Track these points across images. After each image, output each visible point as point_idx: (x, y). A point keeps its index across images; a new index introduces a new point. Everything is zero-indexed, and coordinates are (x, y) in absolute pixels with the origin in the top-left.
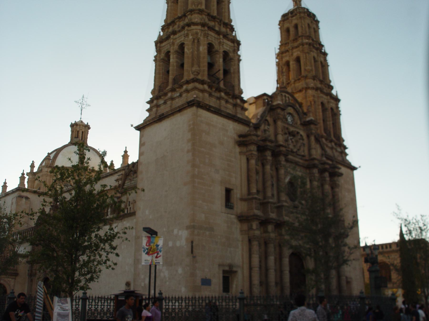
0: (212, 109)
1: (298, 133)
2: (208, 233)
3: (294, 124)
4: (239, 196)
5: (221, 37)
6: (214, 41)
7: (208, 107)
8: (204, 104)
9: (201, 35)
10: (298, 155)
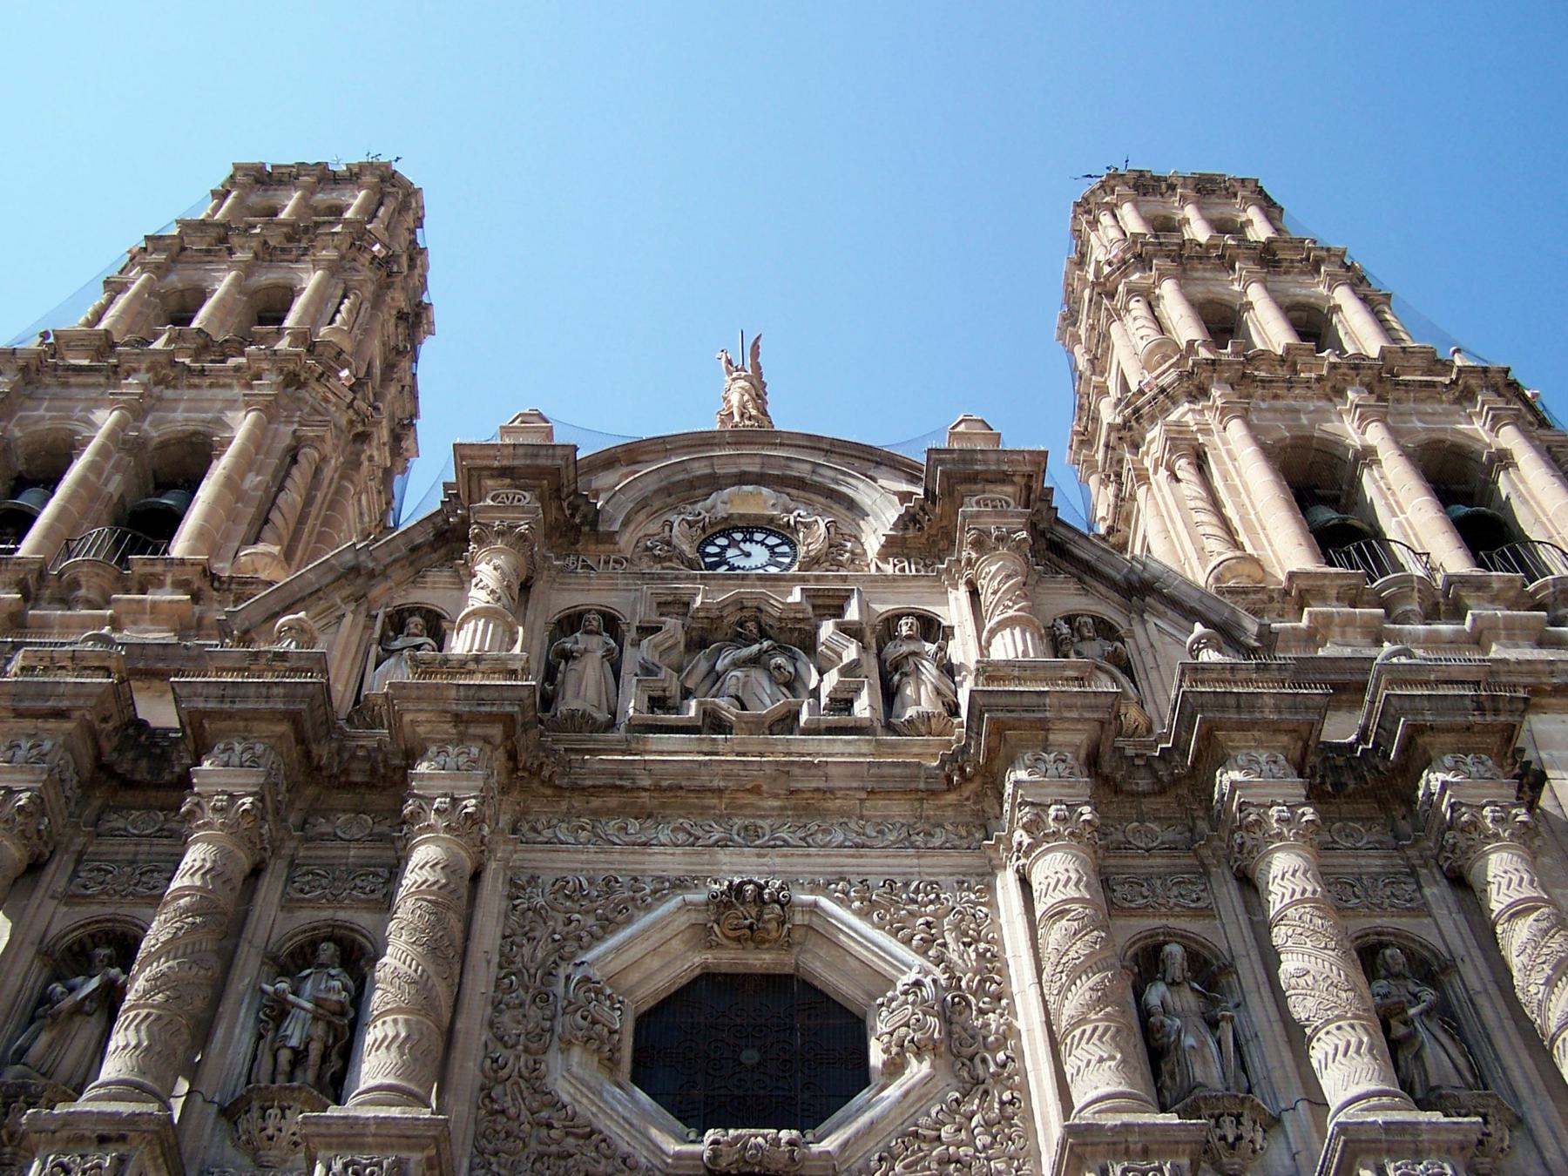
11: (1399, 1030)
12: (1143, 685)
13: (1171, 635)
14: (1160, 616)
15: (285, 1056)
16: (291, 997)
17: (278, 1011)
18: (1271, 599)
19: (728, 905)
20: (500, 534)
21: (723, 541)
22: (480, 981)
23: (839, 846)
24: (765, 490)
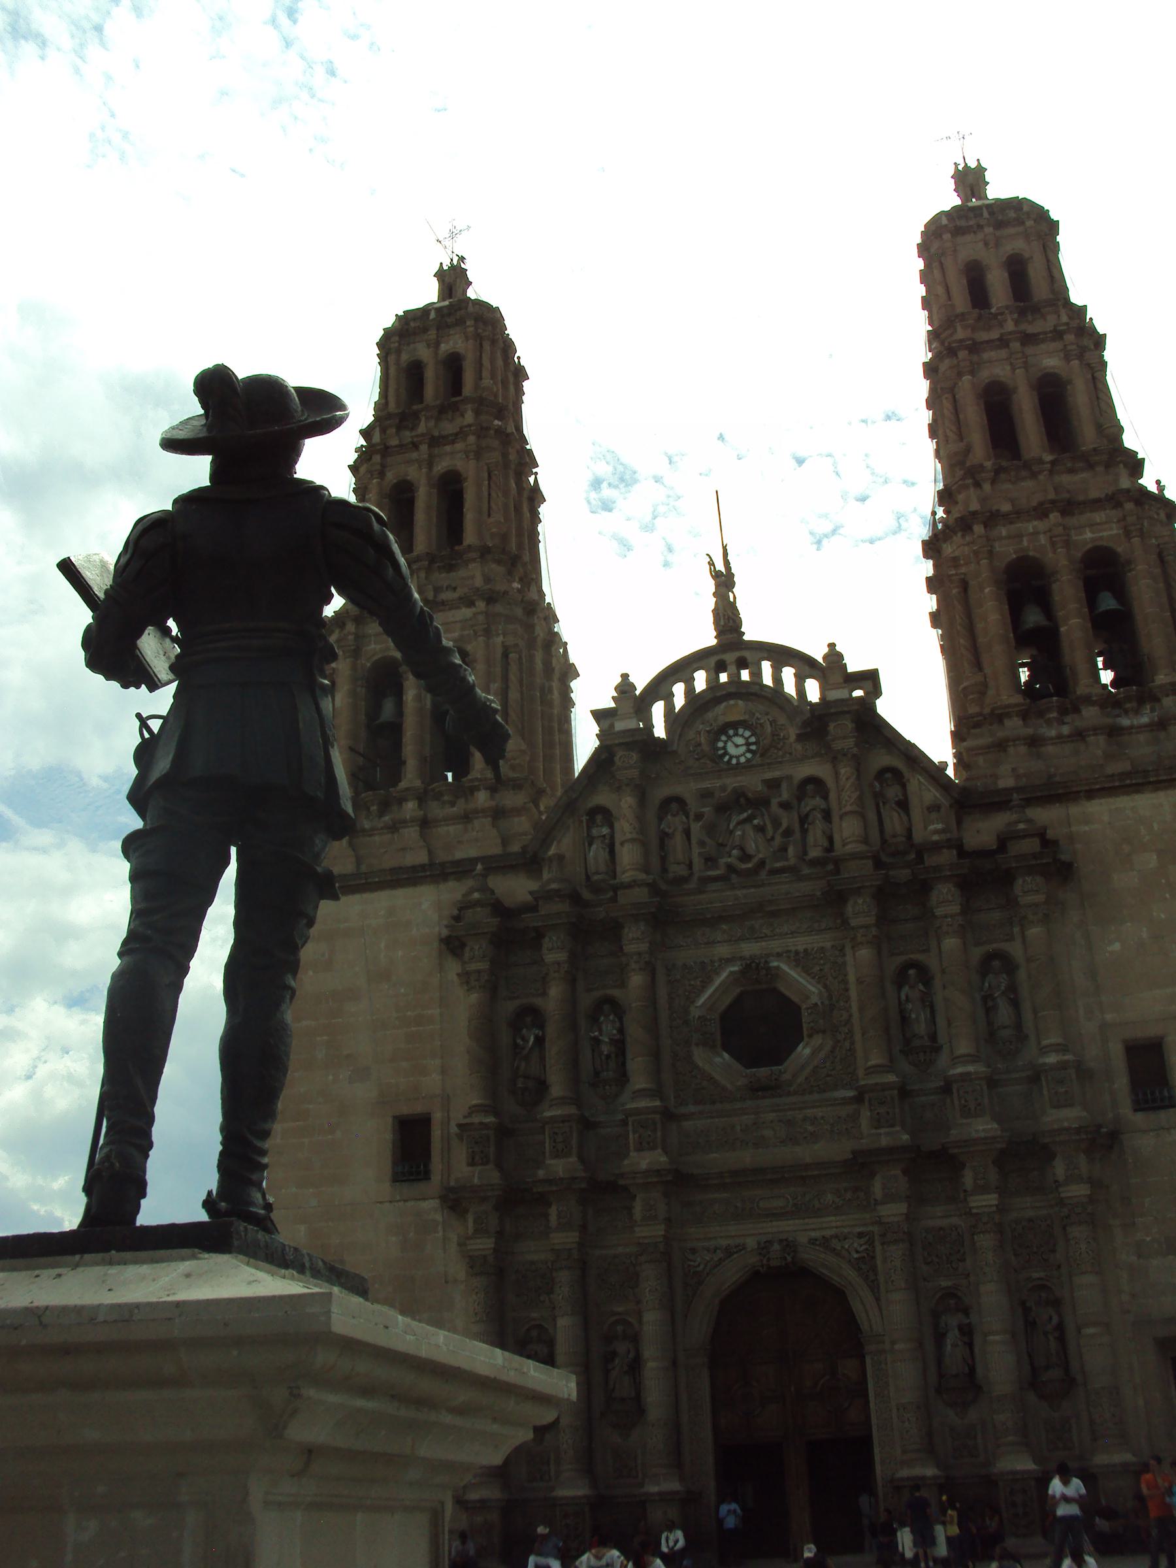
1: (774, 785)
10: (774, 872)
11: (990, 1004)
13: (925, 785)
15: (603, 1058)
16: (601, 1038)
17: (597, 1041)
20: (627, 785)
21: (724, 738)
23: (787, 934)
24: (740, 702)
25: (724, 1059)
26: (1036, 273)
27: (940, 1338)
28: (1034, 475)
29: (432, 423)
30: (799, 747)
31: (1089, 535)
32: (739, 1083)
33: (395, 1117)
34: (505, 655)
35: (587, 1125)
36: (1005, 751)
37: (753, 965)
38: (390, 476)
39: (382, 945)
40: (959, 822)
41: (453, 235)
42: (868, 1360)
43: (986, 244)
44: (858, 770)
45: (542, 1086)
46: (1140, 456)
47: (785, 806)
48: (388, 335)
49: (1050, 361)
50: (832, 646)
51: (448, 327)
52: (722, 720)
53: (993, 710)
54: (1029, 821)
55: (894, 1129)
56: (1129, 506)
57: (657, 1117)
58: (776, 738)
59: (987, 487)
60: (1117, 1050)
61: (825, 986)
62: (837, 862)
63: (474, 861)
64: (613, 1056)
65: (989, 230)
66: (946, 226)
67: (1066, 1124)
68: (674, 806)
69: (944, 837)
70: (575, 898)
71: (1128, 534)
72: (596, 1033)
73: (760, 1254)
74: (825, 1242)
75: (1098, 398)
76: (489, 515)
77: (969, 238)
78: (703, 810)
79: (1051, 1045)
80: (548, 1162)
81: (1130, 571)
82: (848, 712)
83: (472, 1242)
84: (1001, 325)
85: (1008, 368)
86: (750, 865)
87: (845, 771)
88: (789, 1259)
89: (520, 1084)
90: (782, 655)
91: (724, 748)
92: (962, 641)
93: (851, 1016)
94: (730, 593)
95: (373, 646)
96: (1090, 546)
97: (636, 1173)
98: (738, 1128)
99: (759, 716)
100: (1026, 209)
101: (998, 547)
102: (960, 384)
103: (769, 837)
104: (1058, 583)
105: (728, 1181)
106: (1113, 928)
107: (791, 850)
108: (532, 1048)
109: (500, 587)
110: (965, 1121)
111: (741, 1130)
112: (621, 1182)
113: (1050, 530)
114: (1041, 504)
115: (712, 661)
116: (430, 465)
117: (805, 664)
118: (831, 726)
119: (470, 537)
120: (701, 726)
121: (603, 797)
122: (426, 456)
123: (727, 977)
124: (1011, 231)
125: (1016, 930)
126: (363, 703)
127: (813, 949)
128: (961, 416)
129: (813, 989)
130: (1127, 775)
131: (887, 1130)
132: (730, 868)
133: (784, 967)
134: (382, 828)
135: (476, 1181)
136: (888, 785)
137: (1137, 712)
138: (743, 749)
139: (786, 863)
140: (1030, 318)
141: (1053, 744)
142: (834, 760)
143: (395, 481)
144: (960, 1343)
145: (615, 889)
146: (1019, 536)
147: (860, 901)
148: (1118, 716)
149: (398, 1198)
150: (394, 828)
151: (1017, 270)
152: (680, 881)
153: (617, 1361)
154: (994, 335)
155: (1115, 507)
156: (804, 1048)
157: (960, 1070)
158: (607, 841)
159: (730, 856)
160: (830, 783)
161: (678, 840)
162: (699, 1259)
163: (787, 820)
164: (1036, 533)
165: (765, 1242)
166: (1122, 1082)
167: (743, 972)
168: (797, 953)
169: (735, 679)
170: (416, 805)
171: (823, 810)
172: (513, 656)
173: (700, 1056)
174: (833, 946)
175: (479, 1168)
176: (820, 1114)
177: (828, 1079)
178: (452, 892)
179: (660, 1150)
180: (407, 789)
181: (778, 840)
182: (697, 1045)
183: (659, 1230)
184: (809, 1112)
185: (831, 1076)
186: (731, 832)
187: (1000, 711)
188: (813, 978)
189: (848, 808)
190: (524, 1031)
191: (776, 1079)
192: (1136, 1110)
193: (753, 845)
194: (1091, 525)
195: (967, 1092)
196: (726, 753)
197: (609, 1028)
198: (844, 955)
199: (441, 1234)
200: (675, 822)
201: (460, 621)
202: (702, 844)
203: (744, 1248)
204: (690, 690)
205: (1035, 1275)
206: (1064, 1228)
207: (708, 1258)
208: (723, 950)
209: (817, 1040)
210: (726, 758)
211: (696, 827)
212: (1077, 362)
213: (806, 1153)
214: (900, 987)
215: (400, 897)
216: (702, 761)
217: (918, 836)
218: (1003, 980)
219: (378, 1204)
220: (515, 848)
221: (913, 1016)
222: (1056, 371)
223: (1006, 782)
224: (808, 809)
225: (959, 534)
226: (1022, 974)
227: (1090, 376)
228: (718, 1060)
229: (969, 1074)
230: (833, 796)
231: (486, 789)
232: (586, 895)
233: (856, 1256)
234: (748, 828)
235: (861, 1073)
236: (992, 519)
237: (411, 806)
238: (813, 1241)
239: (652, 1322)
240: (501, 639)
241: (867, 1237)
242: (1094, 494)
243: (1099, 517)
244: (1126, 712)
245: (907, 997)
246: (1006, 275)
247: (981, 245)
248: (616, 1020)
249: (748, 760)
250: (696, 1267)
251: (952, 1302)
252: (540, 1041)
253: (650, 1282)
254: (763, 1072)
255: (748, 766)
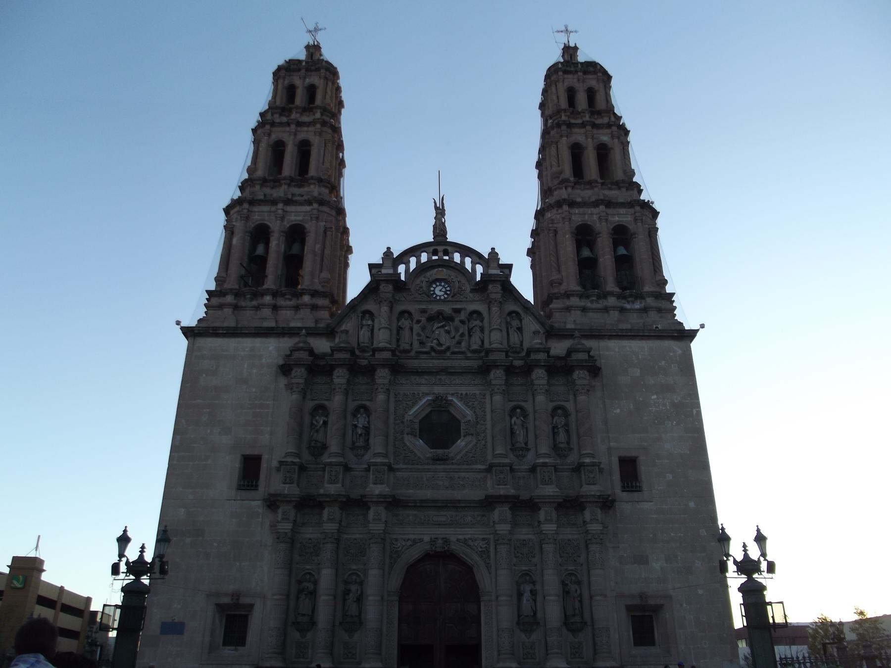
0: (221, 332)
1: (458, 311)
2: (188, 540)
3: (452, 297)
4: (275, 464)
5: (280, 206)
6: (267, 218)
7: (211, 331)
8: (200, 329)
9: (236, 221)
10: (454, 353)
12: (524, 336)
14: (530, 316)
15: (358, 435)
16: (358, 425)
17: (356, 426)
18: (561, 295)
19: (436, 401)
21: (434, 286)
22: (392, 417)
24: (444, 270)
25: (420, 442)
26: (600, 98)
27: (520, 595)
28: (592, 188)
29: (298, 115)
30: (471, 295)
31: (617, 219)
32: (427, 456)
33: (243, 455)
34: (325, 232)
35: (347, 468)
36: (570, 311)
37: (440, 397)
38: (274, 137)
39: (246, 366)
40: (546, 342)
41: (316, 30)
42: (482, 604)
43: (579, 80)
44: (500, 309)
45: (324, 447)
46: (641, 188)
47: (462, 322)
48: (280, 68)
49: (604, 137)
50: (493, 249)
51: (311, 71)
52: (434, 277)
53: (566, 292)
54: (583, 344)
55: (506, 486)
56: (638, 208)
57: (386, 468)
58: (460, 289)
59: (570, 190)
60: (615, 460)
61: (475, 412)
62: (488, 352)
63: (300, 329)
64: (363, 435)
65: (580, 74)
66: (561, 68)
67: (593, 493)
68: (406, 315)
69: (541, 346)
70: (352, 352)
71: (636, 220)
72: (356, 423)
73: (432, 544)
74: (465, 542)
75: (625, 158)
76: (323, 165)
77: (570, 76)
78: (421, 319)
79: (586, 454)
80: (326, 485)
81: (635, 238)
82: (500, 281)
83: (280, 524)
84: (582, 118)
85: (584, 138)
86: (443, 348)
87: (495, 309)
88: (446, 548)
89: (313, 444)
90: (466, 251)
91: (434, 291)
92: (552, 258)
93: (486, 428)
94: (443, 219)
95: (256, 217)
96: (617, 224)
97: (373, 495)
98: (425, 479)
99: (453, 278)
100: (599, 67)
101: (573, 217)
102: (561, 141)
103: (452, 336)
104: (601, 238)
105: (418, 504)
106: (617, 402)
107: (463, 344)
108: (320, 427)
109: (327, 198)
110: (542, 486)
111: (426, 479)
112: (364, 500)
113: (599, 214)
114: (597, 200)
115: (431, 249)
116: (295, 135)
117: (477, 257)
118: (490, 287)
119: (312, 172)
120: (423, 279)
121: (370, 306)
122: (294, 131)
123: (426, 401)
124: (591, 76)
125: (571, 397)
126: (248, 244)
127: (470, 394)
128: (560, 156)
129: (468, 412)
130: (631, 330)
131: (504, 487)
132: (432, 348)
133: (455, 400)
134: (252, 307)
135: (286, 492)
136: (513, 320)
137: (633, 302)
138: (442, 293)
139: (460, 350)
140: (596, 117)
141: (592, 312)
142: (490, 303)
143: (276, 140)
144: (531, 600)
145: (375, 350)
146: (585, 214)
147: (498, 372)
148: (624, 303)
149: (239, 498)
150: (257, 308)
151: (591, 94)
152: (406, 351)
153: (351, 595)
154: (579, 121)
155: (631, 208)
156: (461, 442)
157: (541, 461)
158: (371, 328)
159: (432, 343)
160: (485, 314)
161: (406, 333)
162: (399, 544)
163: (463, 329)
164: (592, 214)
165: (435, 538)
166: (617, 477)
167: (434, 401)
168: (462, 394)
169: (440, 259)
170: (271, 299)
171: (480, 327)
172: (328, 233)
173: (408, 440)
174: (480, 393)
175: (287, 486)
176: (467, 476)
177: (473, 458)
178: (287, 343)
179: (385, 485)
180: (268, 289)
181: (457, 338)
182: (408, 434)
183: (381, 527)
184: (462, 475)
185: (474, 457)
186: (433, 331)
187: (568, 293)
188: (469, 408)
189: (495, 327)
190: (317, 418)
191: (447, 456)
192: (623, 491)
193: (444, 340)
194: (618, 214)
195: (544, 472)
196: (434, 293)
197: (361, 421)
198: (485, 399)
199: (260, 520)
200: (405, 323)
201: (304, 212)
202: (419, 335)
203: (423, 541)
204: (418, 261)
205: (570, 568)
206: (587, 547)
207: (404, 544)
208: (424, 389)
209: (469, 438)
210: (434, 296)
211: (416, 327)
212: (617, 140)
213: (458, 495)
214: (511, 417)
215: (257, 343)
216: (422, 295)
217: (526, 345)
218: (563, 420)
219: (228, 501)
220: (321, 325)
221: (518, 432)
222: (606, 143)
223: (570, 326)
224: (473, 325)
225: (556, 209)
226: (573, 418)
227: (622, 148)
228: (417, 443)
229: (546, 463)
230: (486, 321)
231: (309, 295)
232: (357, 353)
233: (480, 550)
234: (442, 330)
235: (489, 457)
236: (572, 204)
237: (268, 299)
238: (458, 540)
239: (373, 576)
240: (324, 223)
241: (487, 541)
242: (621, 200)
243: (622, 211)
244: (628, 302)
245: (515, 422)
246: (586, 96)
247: (576, 80)
248: (367, 417)
249: (445, 298)
250: (396, 548)
251: (528, 578)
252: (325, 423)
253: (374, 554)
254: (440, 452)
255: (445, 301)
